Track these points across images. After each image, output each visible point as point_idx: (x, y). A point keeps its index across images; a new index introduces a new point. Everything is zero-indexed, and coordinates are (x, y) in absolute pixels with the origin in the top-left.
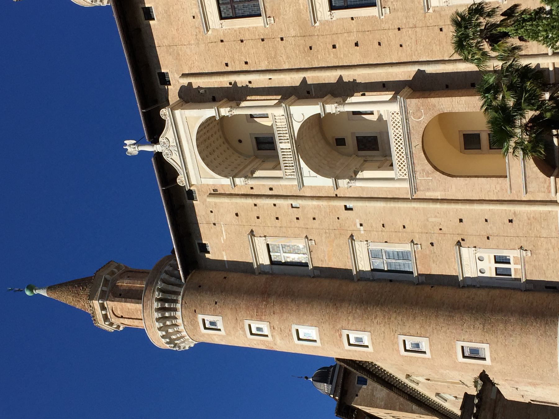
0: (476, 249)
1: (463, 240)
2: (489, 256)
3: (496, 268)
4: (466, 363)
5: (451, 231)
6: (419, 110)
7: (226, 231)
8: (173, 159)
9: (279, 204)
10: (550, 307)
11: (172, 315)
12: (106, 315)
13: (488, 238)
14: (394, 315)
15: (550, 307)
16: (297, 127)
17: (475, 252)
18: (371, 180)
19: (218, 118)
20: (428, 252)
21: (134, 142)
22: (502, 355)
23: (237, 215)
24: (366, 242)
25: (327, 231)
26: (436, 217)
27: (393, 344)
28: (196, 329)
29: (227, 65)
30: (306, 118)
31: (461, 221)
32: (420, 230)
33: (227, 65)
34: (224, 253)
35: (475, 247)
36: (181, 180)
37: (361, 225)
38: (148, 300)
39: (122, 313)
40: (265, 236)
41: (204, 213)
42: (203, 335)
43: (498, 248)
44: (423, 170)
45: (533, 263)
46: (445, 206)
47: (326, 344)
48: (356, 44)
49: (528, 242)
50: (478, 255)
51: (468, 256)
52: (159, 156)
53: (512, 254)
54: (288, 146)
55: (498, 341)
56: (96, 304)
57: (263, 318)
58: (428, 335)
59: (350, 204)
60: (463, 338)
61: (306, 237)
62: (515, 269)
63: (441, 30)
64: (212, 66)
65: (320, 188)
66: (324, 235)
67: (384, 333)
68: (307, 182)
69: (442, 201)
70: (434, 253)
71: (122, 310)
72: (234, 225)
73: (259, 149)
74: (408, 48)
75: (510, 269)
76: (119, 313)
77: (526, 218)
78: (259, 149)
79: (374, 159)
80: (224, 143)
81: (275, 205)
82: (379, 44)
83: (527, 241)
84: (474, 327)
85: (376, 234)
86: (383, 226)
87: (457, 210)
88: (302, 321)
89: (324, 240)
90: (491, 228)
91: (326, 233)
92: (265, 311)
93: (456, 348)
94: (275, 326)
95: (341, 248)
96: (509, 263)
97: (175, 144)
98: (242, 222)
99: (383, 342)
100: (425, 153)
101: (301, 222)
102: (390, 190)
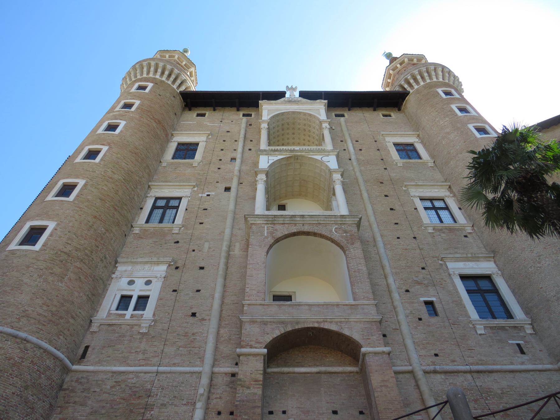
1: (177, 268)
2: (150, 290)
3: (130, 297)
6: (346, 232)
10: (61, 337)
15: (61, 337)
16: (318, 157)
26: (210, 248)
31: (202, 268)
43: (160, 299)
44: (276, 230)
46: (224, 254)
48: (391, 209)
49: (160, 331)
50: (154, 280)
53: (149, 312)
55: (39, 260)
60: (59, 229)
62: (125, 314)
63: (423, 268)
70: (166, 243)
77: (195, 331)
84: (68, 244)
86: (206, 209)
90: (187, 294)
96: (134, 310)
99: (83, 169)
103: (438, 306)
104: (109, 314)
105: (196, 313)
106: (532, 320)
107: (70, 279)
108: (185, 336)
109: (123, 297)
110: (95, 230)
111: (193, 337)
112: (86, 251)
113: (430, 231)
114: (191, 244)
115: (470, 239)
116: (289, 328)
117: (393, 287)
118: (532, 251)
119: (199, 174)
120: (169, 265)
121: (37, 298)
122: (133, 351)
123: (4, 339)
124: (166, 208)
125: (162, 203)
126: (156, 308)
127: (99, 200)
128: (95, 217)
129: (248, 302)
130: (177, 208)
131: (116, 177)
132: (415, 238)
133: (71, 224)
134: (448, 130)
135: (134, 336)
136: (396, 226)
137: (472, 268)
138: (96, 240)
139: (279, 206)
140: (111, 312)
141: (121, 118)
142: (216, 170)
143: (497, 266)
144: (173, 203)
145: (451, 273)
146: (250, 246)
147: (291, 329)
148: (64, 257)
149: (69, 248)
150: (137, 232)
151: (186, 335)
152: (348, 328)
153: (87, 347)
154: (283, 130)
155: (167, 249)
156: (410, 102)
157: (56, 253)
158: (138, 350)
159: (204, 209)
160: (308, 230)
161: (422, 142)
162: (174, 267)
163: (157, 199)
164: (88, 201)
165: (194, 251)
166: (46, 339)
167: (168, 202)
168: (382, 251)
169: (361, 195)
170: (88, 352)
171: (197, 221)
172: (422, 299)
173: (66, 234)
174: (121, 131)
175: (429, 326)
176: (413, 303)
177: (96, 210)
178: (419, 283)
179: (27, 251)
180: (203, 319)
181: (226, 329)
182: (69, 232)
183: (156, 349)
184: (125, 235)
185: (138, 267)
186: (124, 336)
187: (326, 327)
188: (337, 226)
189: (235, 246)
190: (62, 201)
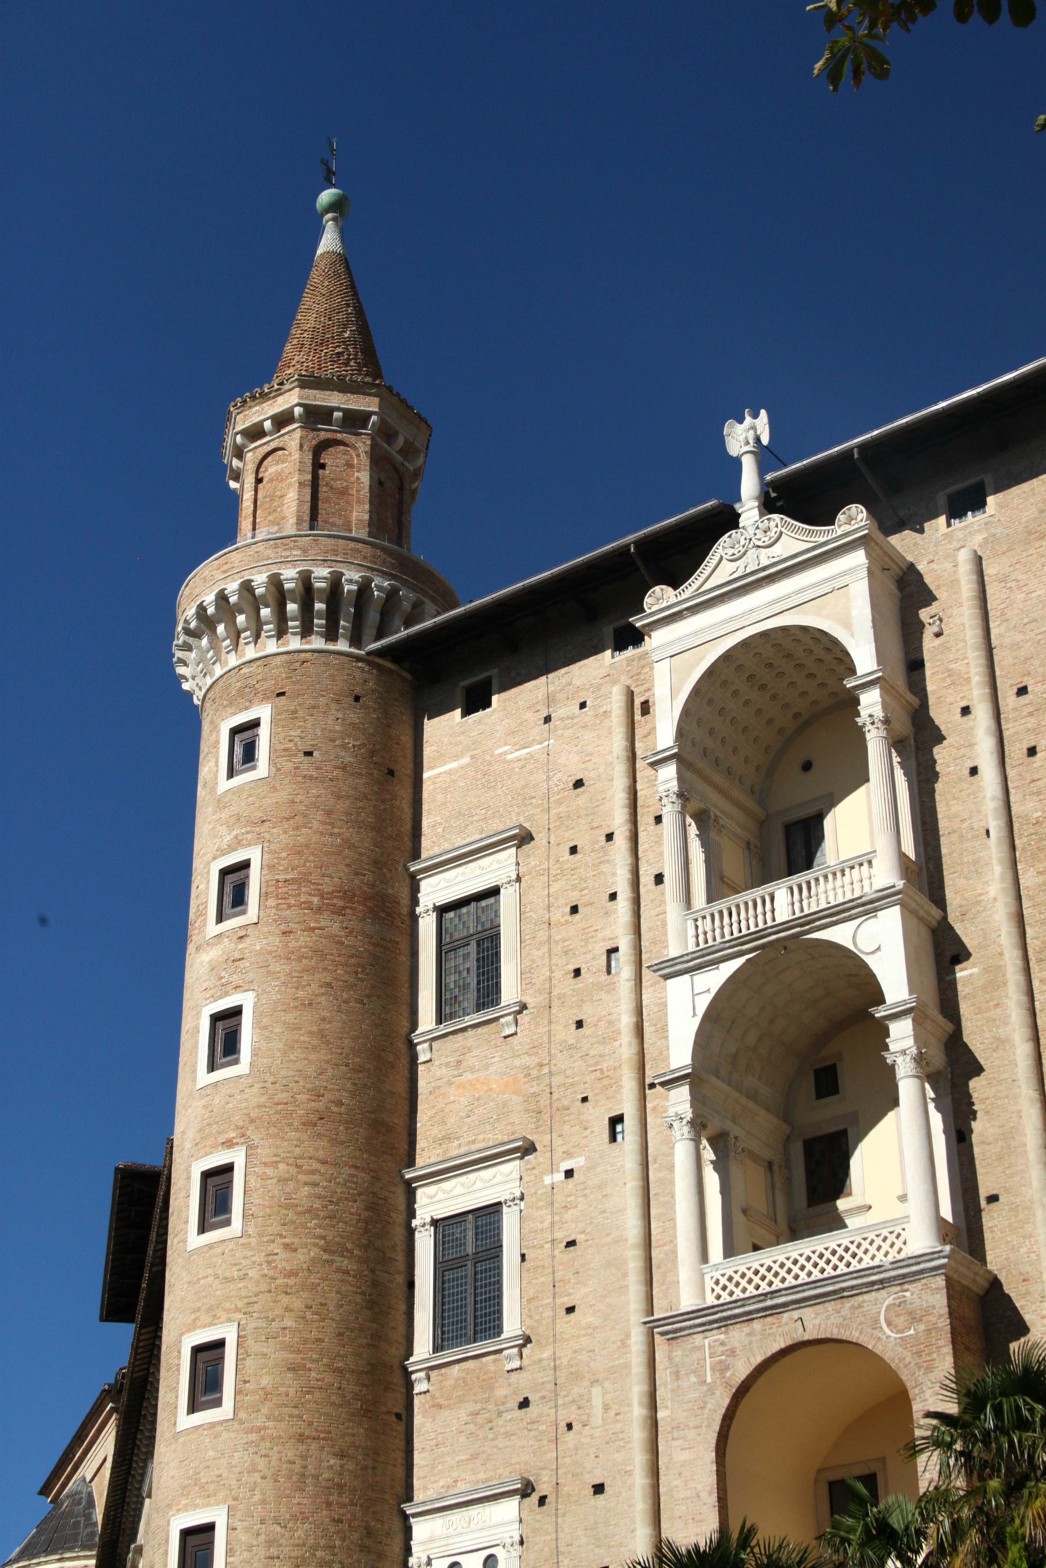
0: (517, 1547)
1: (542, 1501)
4: (167, 1541)
5: (568, 1460)
6: (914, 1318)
7: (531, 756)
8: (721, 564)
9: (615, 911)
11: (265, 627)
12: (262, 434)
14: (298, 1304)
16: (839, 934)
17: (509, 1541)
18: (690, 1185)
19: (850, 683)
20: (501, 1392)
21: (765, 440)
23: (579, 784)
24: (518, 1194)
25: (546, 1070)
26: (606, 1408)
27: (210, 1309)
28: (231, 704)
29: (1022, 691)
30: (871, 961)
31: (599, 1489)
32: (565, 1361)
33: (1022, 691)
34: (466, 760)
35: (522, 1543)
36: (660, 598)
37: (569, 1173)
38: (305, 551)
39: (271, 481)
40: (519, 879)
41: (577, 682)
42: (215, 728)
44: (732, 1352)
46: (638, 1435)
47: (202, 1102)
51: (496, 1520)
52: (726, 520)
54: (783, 914)
56: (290, 399)
57: (271, 902)
58: (242, 1415)
59: (629, 1127)
60: (238, 1524)
61: (524, 1007)
64: (1015, 646)
65: (663, 1030)
66: (531, 1061)
67: (242, 1278)
68: (678, 986)
69: (653, 1424)
70: (500, 1414)
71: (279, 478)
72: (548, 779)
73: (788, 828)
76: (272, 470)
78: (788, 828)
79: (778, 1193)
80: (797, 715)
81: (613, 896)
84: (272, 1558)
85: (546, 1224)
86: (571, 1244)
87: (629, 1473)
88: (266, 1021)
89: (517, 1062)
91: (541, 1065)
92: (289, 906)
93: (209, 1505)
94: (248, 940)
95: (498, 1120)
97: (765, 562)
98: (559, 802)
99: (216, 1276)
100: (783, 1353)
101: (566, 985)
102: (673, 1255)
110: (316, 1477)
112: (320, 1554)
114: (560, 1402)
119: (526, 1070)
128: (301, 1438)
131: (302, 1257)
138: (329, 1505)
139: (818, 1073)
141: (236, 979)
155: (507, 1435)
162: (534, 1498)
164: (267, 1395)
171: (559, 1301)
173: (258, 1535)
174: (255, 1053)
177: (296, 1412)
184: (398, 1416)
190: (213, 1425)
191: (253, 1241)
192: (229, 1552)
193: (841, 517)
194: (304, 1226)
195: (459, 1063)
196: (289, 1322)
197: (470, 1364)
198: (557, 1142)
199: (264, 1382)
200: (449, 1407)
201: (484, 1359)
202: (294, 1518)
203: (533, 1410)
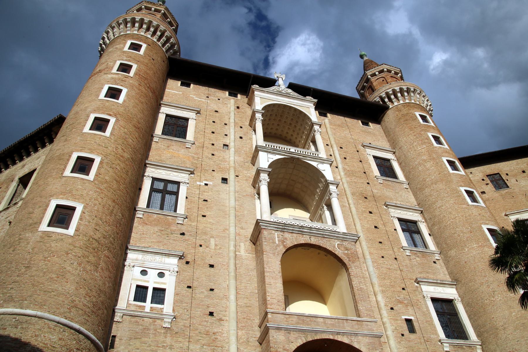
1: (187, 263)
3: (146, 288)
6: (347, 249)
13: (189, 287)
14: (122, 165)
20: (174, 228)
22: (53, 245)
26: (216, 245)
30: (322, 171)
31: (212, 266)
32: (201, 228)
34: (181, 93)
37: (206, 184)
43: (176, 294)
44: (286, 239)
45: (152, 327)
46: (232, 255)
48: (376, 227)
50: (167, 273)
53: (168, 307)
55: (75, 247)
63: (403, 289)
70: (172, 234)
74: (381, 262)
75: (144, 301)
77: (215, 330)
82: (380, 242)
83: (185, 326)
84: (96, 230)
86: (206, 201)
90: (202, 292)
103: (415, 324)
104: (128, 304)
105: (213, 313)
106: (482, 342)
107: (102, 269)
108: (206, 335)
109: (138, 286)
111: (213, 337)
113: (408, 254)
115: (437, 266)
116: (310, 339)
117: (382, 304)
118: (488, 286)
120: (180, 259)
121: (81, 288)
122: (159, 345)
123: (62, 330)
124: (164, 192)
125: (160, 186)
126: (174, 303)
127: (115, 181)
128: (114, 201)
129: (272, 310)
130: (176, 194)
132: (396, 259)
133: (96, 208)
134: (425, 158)
135: (158, 330)
136: (380, 245)
137: (440, 293)
140: (130, 302)
142: (210, 156)
143: (458, 292)
144: (171, 188)
145: (425, 295)
146: (265, 253)
147: (311, 340)
148: (96, 245)
149: (98, 236)
150: (141, 216)
151: (207, 333)
152: (357, 342)
153: (114, 337)
154: (270, 119)
155: (174, 240)
156: (390, 116)
157: (89, 240)
158: (165, 345)
159: (204, 200)
160: (314, 243)
161: (398, 160)
162: (184, 261)
163: (154, 179)
165: (201, 246)
166: (91, 330)
167: (166, 186)
168: (371, 269)
169: (350, 208)
170: (116, 343)
172: (404, 317)
173: (93, 219)
175: (409, 341)
176: (397, 320)
178: (401, 302)
179: (62, 235)
180: (221, 320)
181: (244, 331)
182: (96, 217)
183: (181, 345)
185: (149, 257)
186: (148, 329)
187: (340, 340)
188: (339, 243)
189: (240, 246)
191: (112, 141)
192: (81, 219)
193: (307, 97)
194: (128, 148)
195: (168, 147)
196: (117, 167)
197: (162, 217)
198: (202, 176)
199: (107, 178)
200: (150, 225)
201: (168, 217)
202: (106, 222)
203: (185, 237)
